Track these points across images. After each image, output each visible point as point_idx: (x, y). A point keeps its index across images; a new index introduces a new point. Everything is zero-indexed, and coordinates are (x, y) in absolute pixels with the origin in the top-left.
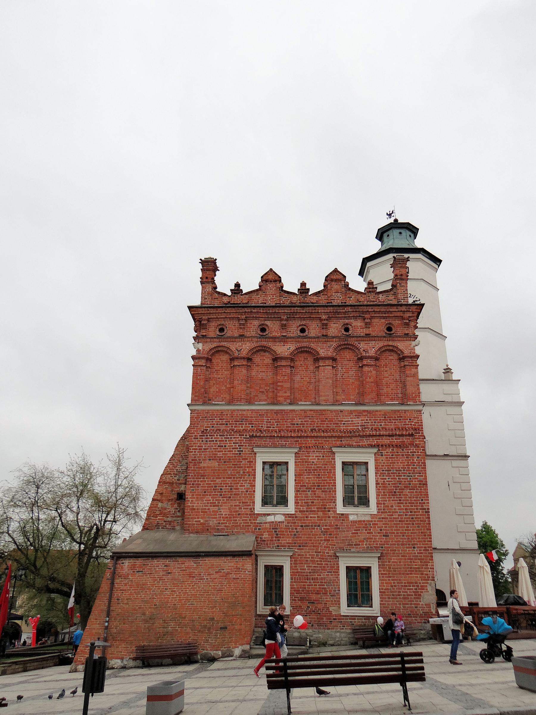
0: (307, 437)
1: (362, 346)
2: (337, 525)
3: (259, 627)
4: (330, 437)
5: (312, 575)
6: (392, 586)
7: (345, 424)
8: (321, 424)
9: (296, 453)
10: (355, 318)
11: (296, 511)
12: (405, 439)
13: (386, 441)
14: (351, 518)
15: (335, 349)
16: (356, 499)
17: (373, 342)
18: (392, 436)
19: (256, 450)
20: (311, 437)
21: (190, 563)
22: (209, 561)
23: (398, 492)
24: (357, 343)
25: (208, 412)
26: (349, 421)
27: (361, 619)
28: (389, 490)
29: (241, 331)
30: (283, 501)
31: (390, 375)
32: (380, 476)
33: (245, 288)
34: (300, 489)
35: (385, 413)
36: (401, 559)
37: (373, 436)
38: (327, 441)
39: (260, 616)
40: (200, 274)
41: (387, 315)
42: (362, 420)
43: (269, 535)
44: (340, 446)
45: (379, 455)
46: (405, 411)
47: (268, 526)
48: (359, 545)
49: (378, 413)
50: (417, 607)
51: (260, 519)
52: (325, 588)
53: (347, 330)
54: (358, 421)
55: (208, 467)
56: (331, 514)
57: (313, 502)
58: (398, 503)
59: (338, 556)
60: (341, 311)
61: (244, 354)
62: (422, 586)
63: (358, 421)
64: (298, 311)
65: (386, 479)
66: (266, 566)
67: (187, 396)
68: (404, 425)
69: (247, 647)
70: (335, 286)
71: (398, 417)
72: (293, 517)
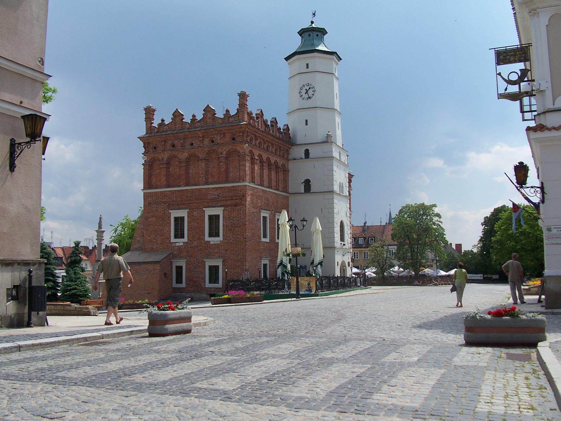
14: (211, 243)
16: (214, 234)
18: (232, 200)
19: (170, 211)
22: (143, 266)
25: (150, 193)
30: (182, 236)
33: (166, 123)
35: (229, 188)
40: (144, 116)
44: (207, 207)
46: (238, 186)
51: (173, 245)
53: (213, 142)
54: (216, 193)
63: (216, 193)
66: (176, 266)
67: (141, 185)
69: (157, 301)
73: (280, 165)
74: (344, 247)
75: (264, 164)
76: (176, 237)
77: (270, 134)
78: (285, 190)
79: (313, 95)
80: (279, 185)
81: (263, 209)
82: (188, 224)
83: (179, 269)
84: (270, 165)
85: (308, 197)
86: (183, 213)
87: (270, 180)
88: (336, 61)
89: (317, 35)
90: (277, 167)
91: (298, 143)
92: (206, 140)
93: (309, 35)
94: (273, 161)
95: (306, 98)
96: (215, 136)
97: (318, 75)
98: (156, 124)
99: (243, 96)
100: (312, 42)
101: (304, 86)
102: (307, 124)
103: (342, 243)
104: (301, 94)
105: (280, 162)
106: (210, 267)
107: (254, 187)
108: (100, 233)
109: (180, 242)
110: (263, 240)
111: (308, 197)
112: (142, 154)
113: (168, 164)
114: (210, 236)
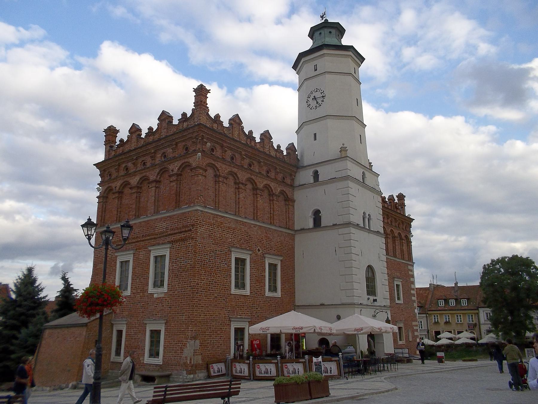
0: (140, 241)
1: (171, 167)
2: (148, 302)
3: (112, 369)
4: (151, 239)
5: (134, 336)
6: (170, 344)
7: (157, 228)
8: (147, 231)
9: (134, 254)
11: (131, 294)
12: (187, 234)
13: (178, 237)
14: (155, 296)
18: (181, 232)
20: (143, 241)
23: (179, 275)
24: (169, 165)
26: (160, 226)
27: (153, 366)
28: (175, 273)
29: (117, 173)
31: (187, 185)
32: (171, 264)
34: (134, 278)
36: (176, 324)
37: (172, 234)
38: (150, 242)
39: (112, 362)
41: (184, 139)
42: (167, 224)
43: (119, 310)
45: (172, 249)
46: (189, 212)
48: (157, 315)
49: (175, 217)
50: (180, 359)
52: (139, 345)
53: (165, 157)
55: (100, 268)
57: (139, 287)
58: (179, 283)
60: (159, 144)
62: (185, 344)
64: (139, 151)
65: (173, 266)
68: (187, 223)
69: (74, 383)
71: (185, 218)
72: (129, 298)
74: (376, 304)
79: (323, 101)
80: (273, 218)
82: (133, 270)
85: (318, 235)
89: (330, 32)
90: (271, 194)
93: (320, 33)
94: (261, 186)
101: (312, 93)
102: (315, 139)
103: (372, 298)
104: (309, 103)
105: (277, 189)
106: (152, 331)
112: (98, 184)
113: (121, 192)
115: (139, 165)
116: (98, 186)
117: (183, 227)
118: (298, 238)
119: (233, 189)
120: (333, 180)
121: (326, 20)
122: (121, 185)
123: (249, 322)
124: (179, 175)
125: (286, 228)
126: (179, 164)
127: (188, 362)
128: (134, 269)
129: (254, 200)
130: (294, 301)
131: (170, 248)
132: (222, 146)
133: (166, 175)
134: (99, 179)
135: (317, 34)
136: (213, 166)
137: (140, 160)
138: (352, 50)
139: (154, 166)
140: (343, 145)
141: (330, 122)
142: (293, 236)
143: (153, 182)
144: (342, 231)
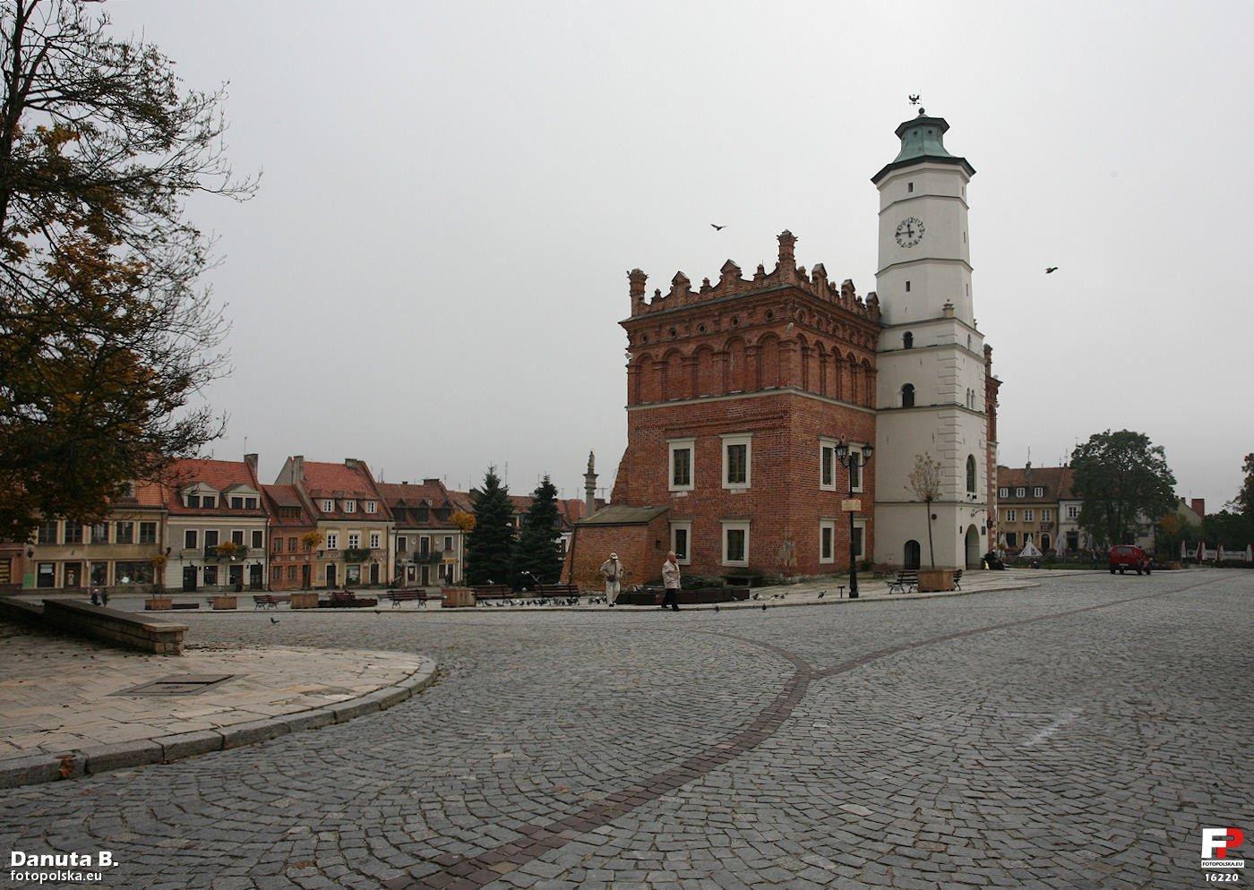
1: (747, 337)
4: (721, 425)
10: (742, 309)
12: (777, 422)
13: (762, 425)
14: (732, 492)
15: (726, 343)
17: (756, 331)
20: (707, 426)
21: (614, 531)
22: (625, 529)
30: (687, 482)
33: (663, 296)
35: (762, 399)
40: (629, 288)
47: (677, 500)
51: (673, 495)
53: (736, 322)
54: (742, 408)
56: (718, 490)
59: (722, 523)
61: (660, 359)
70: (730, 278)
73: (859, 361)
75: (827, 358)
76: (677, 482)
77: (840, 308)
78: (869, 404)
79: (921, 237)
81: (824, 435)
83: (681, 534)
84: (839, 360)
86: (689, 445)
87: (839, 387)
88: (963, 175)
90: (854, 365)
91: (894, 321)
92: (725, 320)
94: (844, 355)
95: (907, 244)
96: (739, 312)
97: (929, 201)
98: (648, 301)
99: (787, 241)
100: (920, 145)
102: (908, 289)
107: (807, 398)
108: (591, 476)
109: (683, 491)
110: (823, 487)
111: (910, 418)
114: (731, 480)
115: (694, 329)
116: (627, 351)
117: (771, 413)
118: (880, 419)
119: (818, 363)
120: (933, 347)
121: (922, 111)
122: (665, 354)
123: (835, 522)
124: (758, 348)
125: (867, 407)
126: (762, 333)
127: (786, 564)
128: (696, 459)
129: (837, 375)
130: (874, 498)
131: (752, 437)
132: (810, 310)
133: (738, 346)
134: (627, 343)
135: (910, 133)
136: (801, 336)
137: (696, 324)
138: (964, 164)
139: (718, 333)
140: (948, 301)
141: (929, 267)
142: (874, 416)
143: (718, 353)
144: (943, 413)
